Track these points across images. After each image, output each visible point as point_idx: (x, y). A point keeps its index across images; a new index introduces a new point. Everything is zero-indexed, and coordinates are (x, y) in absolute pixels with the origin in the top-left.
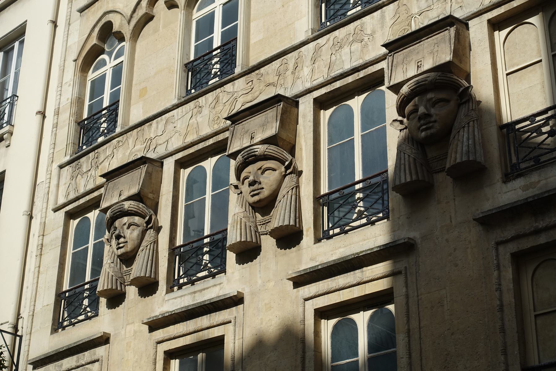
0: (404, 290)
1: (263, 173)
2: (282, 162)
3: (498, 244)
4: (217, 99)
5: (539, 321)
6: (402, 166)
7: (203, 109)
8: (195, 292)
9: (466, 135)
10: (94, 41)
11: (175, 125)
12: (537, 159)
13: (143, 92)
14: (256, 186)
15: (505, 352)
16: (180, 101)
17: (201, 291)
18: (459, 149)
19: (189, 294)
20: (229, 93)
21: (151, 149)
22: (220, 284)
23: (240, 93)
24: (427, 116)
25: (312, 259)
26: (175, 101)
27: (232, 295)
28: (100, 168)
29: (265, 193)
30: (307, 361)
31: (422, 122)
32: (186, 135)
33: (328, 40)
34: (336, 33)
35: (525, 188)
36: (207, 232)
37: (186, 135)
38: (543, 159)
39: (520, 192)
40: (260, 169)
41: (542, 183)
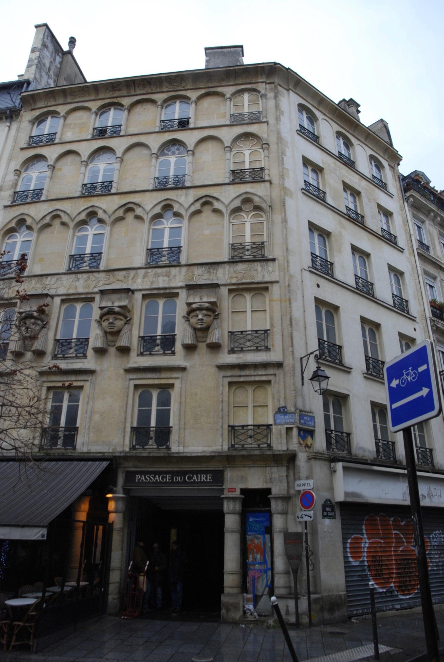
0: (180, 386)
1: (116, 320)
2: (126, 317)
3: (224, 377)
4: (89, 278)
5: (235, 408)
6: (187, 337)
7: (80, 280)
8: (68, 363)
9: (217, 332)
10: (13, 225)
11: (62, 282)
12: (242, 348)
13: (41, 260)
14: (112, 325)
15: (222, 418)
16: (67, 272)
17: (72, 363)
18: (214, 336)
19: (66, 363)
20: (95, 277)
21: (46, 289)
22: (83, 362)
23: (102, 279)
24: (202, 320)
25: (135, 363)
26: (64, 271)
27: (92, 369)
28: (12, 289)
29: (116, 329)
30: (128, 405)
31: (200, 321)
32: (69, 289)
33: (152, 271)
34: (157, 269)
35: (237, 358)
36: (74, 336)
37: (69, 289)
38: (244, 349)
39: (235, 359)
40: (115, 318)
41: (244, 358)
